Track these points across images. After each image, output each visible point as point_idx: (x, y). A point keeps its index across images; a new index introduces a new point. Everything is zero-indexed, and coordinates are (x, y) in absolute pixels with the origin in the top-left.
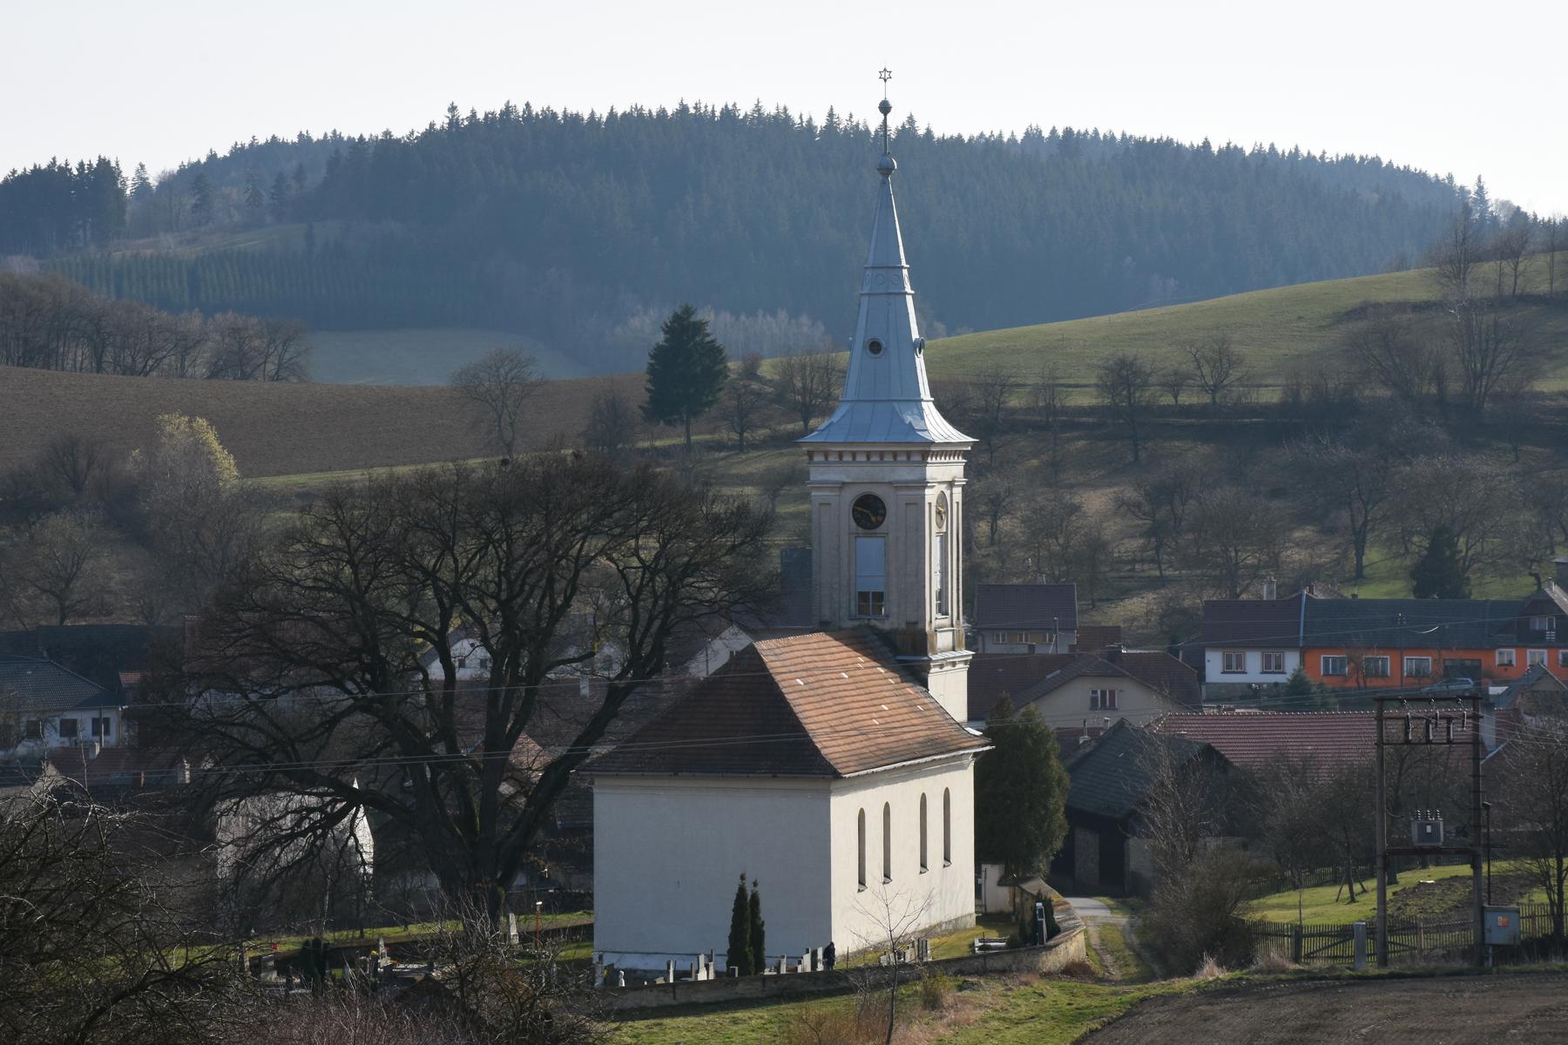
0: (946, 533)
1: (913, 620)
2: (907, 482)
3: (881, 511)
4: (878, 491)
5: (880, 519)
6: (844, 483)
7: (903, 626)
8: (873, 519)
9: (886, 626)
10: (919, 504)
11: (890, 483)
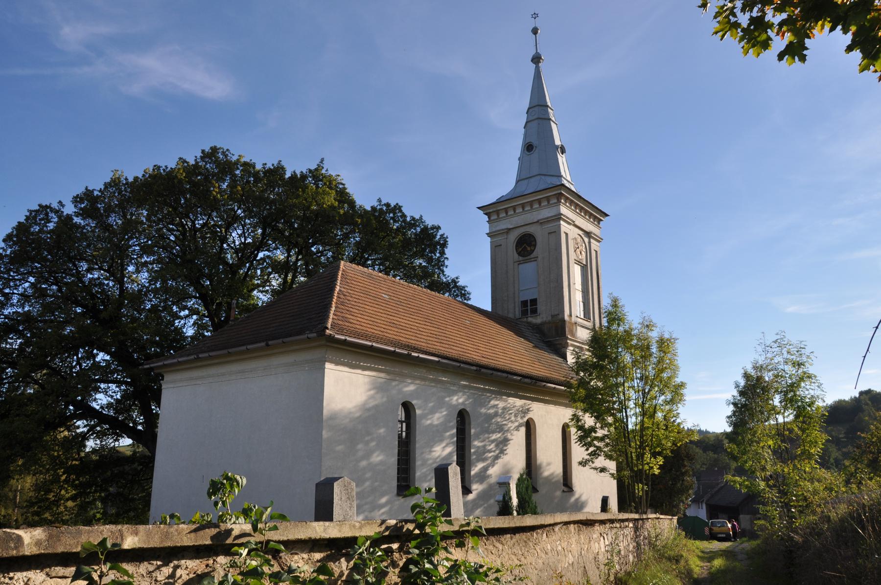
0: (586, 265)
1: (556, 313)
2: (548, 218)
3: (533, 243)
4: (531, 230)
5: (533, 248)
6: (510, 229)
7: (550, 318)
8: (529, 249)
9: (537, 320)
10: (557, 232)
11: (538, 222)
